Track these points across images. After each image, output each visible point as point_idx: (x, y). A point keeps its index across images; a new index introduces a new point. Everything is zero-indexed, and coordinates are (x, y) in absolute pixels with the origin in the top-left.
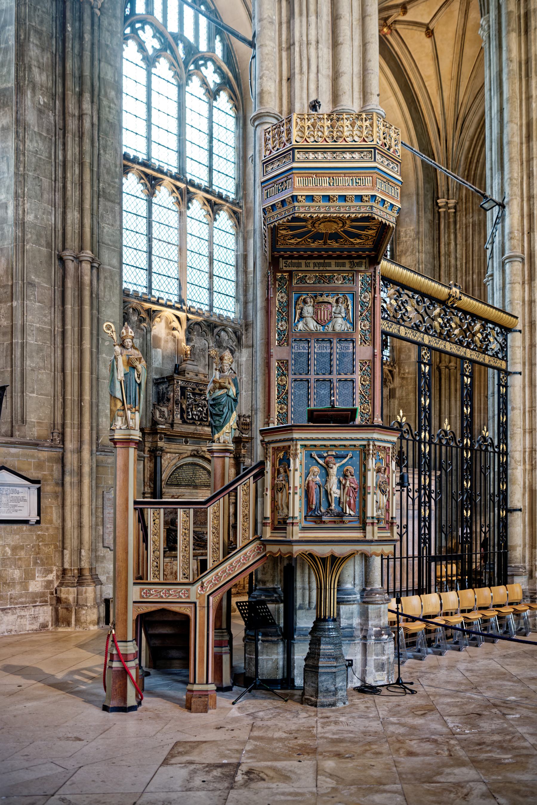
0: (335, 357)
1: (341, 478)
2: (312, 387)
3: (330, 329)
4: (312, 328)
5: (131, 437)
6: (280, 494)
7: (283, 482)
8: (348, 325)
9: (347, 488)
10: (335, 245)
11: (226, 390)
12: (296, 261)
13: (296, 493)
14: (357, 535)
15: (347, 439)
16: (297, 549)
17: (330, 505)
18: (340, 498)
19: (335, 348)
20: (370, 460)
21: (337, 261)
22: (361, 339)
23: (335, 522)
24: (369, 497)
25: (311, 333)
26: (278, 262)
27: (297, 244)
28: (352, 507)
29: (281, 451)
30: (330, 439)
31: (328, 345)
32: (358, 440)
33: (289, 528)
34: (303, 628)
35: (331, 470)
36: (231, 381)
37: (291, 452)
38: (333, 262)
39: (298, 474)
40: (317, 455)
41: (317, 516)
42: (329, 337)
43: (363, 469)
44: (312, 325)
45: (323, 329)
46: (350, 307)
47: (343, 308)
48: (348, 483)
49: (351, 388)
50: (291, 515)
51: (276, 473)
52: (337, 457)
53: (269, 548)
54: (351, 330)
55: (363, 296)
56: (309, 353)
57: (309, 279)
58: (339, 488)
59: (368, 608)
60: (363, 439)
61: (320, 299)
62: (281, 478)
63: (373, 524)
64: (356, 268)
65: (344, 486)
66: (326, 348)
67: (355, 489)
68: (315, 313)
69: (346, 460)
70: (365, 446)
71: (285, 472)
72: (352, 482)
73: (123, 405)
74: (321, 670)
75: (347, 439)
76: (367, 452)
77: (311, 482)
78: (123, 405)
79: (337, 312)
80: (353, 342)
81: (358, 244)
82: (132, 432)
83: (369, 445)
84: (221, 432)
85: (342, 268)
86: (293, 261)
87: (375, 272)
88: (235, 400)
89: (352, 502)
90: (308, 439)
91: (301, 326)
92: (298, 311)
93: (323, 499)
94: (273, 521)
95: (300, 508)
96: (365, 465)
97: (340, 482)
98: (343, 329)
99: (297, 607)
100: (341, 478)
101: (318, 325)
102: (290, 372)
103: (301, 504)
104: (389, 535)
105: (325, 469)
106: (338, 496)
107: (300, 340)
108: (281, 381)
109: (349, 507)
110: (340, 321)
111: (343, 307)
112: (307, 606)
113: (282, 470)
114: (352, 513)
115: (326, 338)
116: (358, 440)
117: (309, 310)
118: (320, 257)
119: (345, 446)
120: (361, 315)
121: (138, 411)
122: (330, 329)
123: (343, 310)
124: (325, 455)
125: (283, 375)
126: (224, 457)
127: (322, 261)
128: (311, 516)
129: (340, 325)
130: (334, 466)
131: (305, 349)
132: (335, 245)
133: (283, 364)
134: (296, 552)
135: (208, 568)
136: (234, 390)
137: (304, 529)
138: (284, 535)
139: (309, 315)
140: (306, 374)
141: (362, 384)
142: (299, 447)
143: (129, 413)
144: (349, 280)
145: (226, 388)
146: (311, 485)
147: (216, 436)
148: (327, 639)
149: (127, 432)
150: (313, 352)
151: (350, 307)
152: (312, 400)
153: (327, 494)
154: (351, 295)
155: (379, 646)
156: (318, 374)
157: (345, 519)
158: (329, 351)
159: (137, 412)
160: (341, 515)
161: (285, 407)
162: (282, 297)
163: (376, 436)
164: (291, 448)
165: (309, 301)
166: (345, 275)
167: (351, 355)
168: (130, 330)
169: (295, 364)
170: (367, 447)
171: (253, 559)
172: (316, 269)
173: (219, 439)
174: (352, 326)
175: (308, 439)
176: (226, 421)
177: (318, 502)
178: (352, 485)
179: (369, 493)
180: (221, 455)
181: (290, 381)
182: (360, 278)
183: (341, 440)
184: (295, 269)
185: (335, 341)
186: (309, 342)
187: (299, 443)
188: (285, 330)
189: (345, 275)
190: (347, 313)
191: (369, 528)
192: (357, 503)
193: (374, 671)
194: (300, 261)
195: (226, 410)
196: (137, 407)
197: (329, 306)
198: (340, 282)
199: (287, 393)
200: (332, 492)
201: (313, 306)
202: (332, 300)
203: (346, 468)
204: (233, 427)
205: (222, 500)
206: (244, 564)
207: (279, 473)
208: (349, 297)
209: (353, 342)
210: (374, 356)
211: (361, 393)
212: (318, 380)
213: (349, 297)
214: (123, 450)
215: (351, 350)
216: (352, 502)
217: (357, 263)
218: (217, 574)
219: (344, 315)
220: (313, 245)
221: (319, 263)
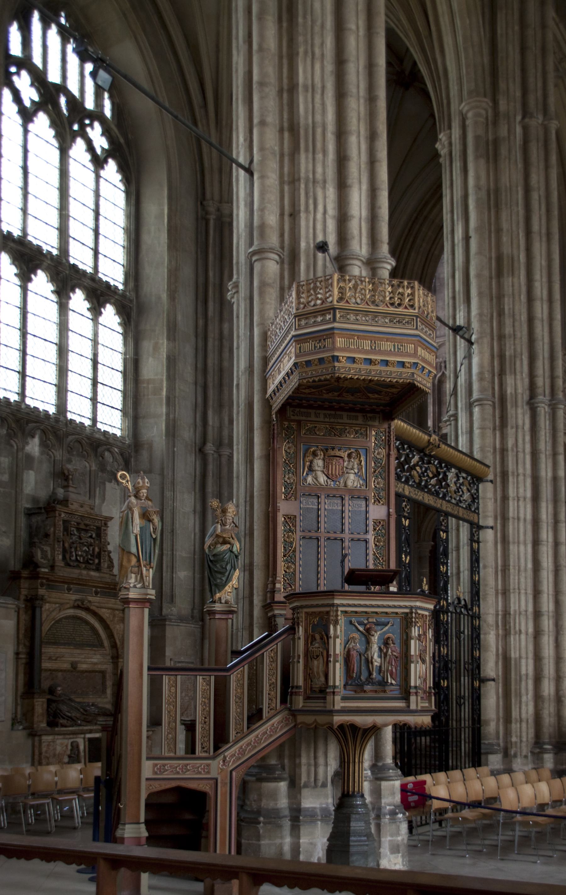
0: (346, 514)
1: (382, 646)
2: (322, 546)
4: (322, 482)
6: (316, 662)
7: (321, 649)
8: (361, 482)
9: (388, 657)
10: (350, 398)
11: (229, 546)
12: (305, 410)
13: (338, 661)
14: (400, 704)
15: (389, 607)
16: (338, 719)
17: (370, 674)
18: (380, 667)
19: (347, 505)
20: (413, 629)
21: (349, 414)
22: (375, 496)
23: (376, 691)
24: (413, 666)
25: (321, 488)
27: (309, 394)
28: (394, 676)
29: (316, 617)
30: (372, 606)
32: (400, 607)
33: (329, 698)
34: (309, 808)
35: (373, 638)
37: (332, 618)
38: (345, 414)
39: (338, 641)
41: (357, 685)
42: (340, 493)
43: (405, 637)
44: (322, 479)
45: (334, 486)
46: (363, 463)
47: (356, 463)
48: (390, 651)
49: (364, 548)
50: (331, 683)
51: (310, 639)
52: (377, 624)
53: (301, 718)
54: (363, 488)
55: (377, 452)
56: (318, 509)
58: (380, 657)
59: (380, 785)
60: (406, 607)
61: (332, 453)
62: (317, 645)
63: (416, 694)
64: (370, 423)
65: (386, 655)
66: (337, 504)
67: (397, 657)
68: (326, 466)
69: (387, 628)
70: (407, 613)
71: (322, 638)
72: (395, 649)
74: (352, 850)
75: (389, 607)
76: (409, 620)
77: (352, 650)
80: (366, 500)
81: (376, 399)
83: (412, 613)
84: (223, 592)
85: (354, 422)
86: (302, 410)
87: (389, 428)
89: (394, 670)
90: (349, 606)
91: (310, 479)
92: (308, 463)
93: (363, 668)
94: (305, 690)
95: (340, 676)
96: (407, 634)
97: (380, 649)
99: (302, 784)
100: (382, 646)
101: (328, 480)
103: (340, 673)
104: (427, 705)
105: (365, 636)
106: (378, 665)
107: (309, 495)
108: (288, 537)
109: (391, 677)
110: (352, 476)
111: (356, 462)
112: (313, 784)
113: (317, 636)
114: (393, 682)
115: (338, 493)
116: (400, 607)
117: (319, 463)
118: (331, 408)
119: (386, 613)
120: (374, 472)
121: (152, 568)
122: (342, 484)
123: (356, 466)
124: (366, 622)
125: (290, 531)
126: (227, 619)
127: (333, 412)
128: (351, 685)
129: (352, 480)
130: (375, 634)
131: (314, 505)
132: (350, 398)
133: (290, 519)
134: (336, 723)
135: (231, 741)
136: (238, 546)
137: (344, 699)
138: (322, 705)
139: (319, 469)
140: (316, 532)
141: (376, 545)
142: (339, 613)
143: (144, 569)
144: (361, 434)
145: (229, 543)
146: (352, 653)
147: (218, 595)
148: (357, 816)
149: (143, 591)
150: (323, 509)
151: (363, 463)
152: (322, 559)
153: (369, 662)
154: (364, 451)
155: (394, 826)
156: (328, 532)
157: (388, 688)
160: (383, 683)
161: (293, 566)
162: (289, 448)
163: (418, 604)
164: (331, 614)
165: (319, 454)
166: (357, 429)
167: (364, 513)
168: (146, 480)
169: (303, 520)
170: (409, 615)
171: (281, 730)
172: (327, 420)
173: (220, 599)
174: (365, 483)
175: (349, 606)
176: (229, 579)
177: (359, 670)
178: (395, 654)
179: (413, 662)
180: (224, 617)
181: (298, 538)
182: (373, 433)
183: (384, 606)
184: (304, 418)
185: (347, 498)
186: (318, 497)
187: (340, 609)
188: (292, 483)
189: (357, 429)
190: (360, 469)
191: (413, 698)
192: (398, 672)
193: (388, 853)
195: (229, 567)
197: (341, 461)
198: (352, 436)
199: (294, 551)
200: (374, 660)
201: (324, 460)
203: (386, 636)
204: (235, 586)
205: (246, 667)
206: (271, 736)
207: (314, 639)
208: (362, 452)
209: (366, 500)
210: (389, 515)
211: (374, 554)
212: (329, 539)
213: (362, 452)
214: (137, 610)
216: (394, 670)
217: (370, 417)
218: (241, 747)
219: (356, 471)
220: (325, 396)
221: (330, 415)
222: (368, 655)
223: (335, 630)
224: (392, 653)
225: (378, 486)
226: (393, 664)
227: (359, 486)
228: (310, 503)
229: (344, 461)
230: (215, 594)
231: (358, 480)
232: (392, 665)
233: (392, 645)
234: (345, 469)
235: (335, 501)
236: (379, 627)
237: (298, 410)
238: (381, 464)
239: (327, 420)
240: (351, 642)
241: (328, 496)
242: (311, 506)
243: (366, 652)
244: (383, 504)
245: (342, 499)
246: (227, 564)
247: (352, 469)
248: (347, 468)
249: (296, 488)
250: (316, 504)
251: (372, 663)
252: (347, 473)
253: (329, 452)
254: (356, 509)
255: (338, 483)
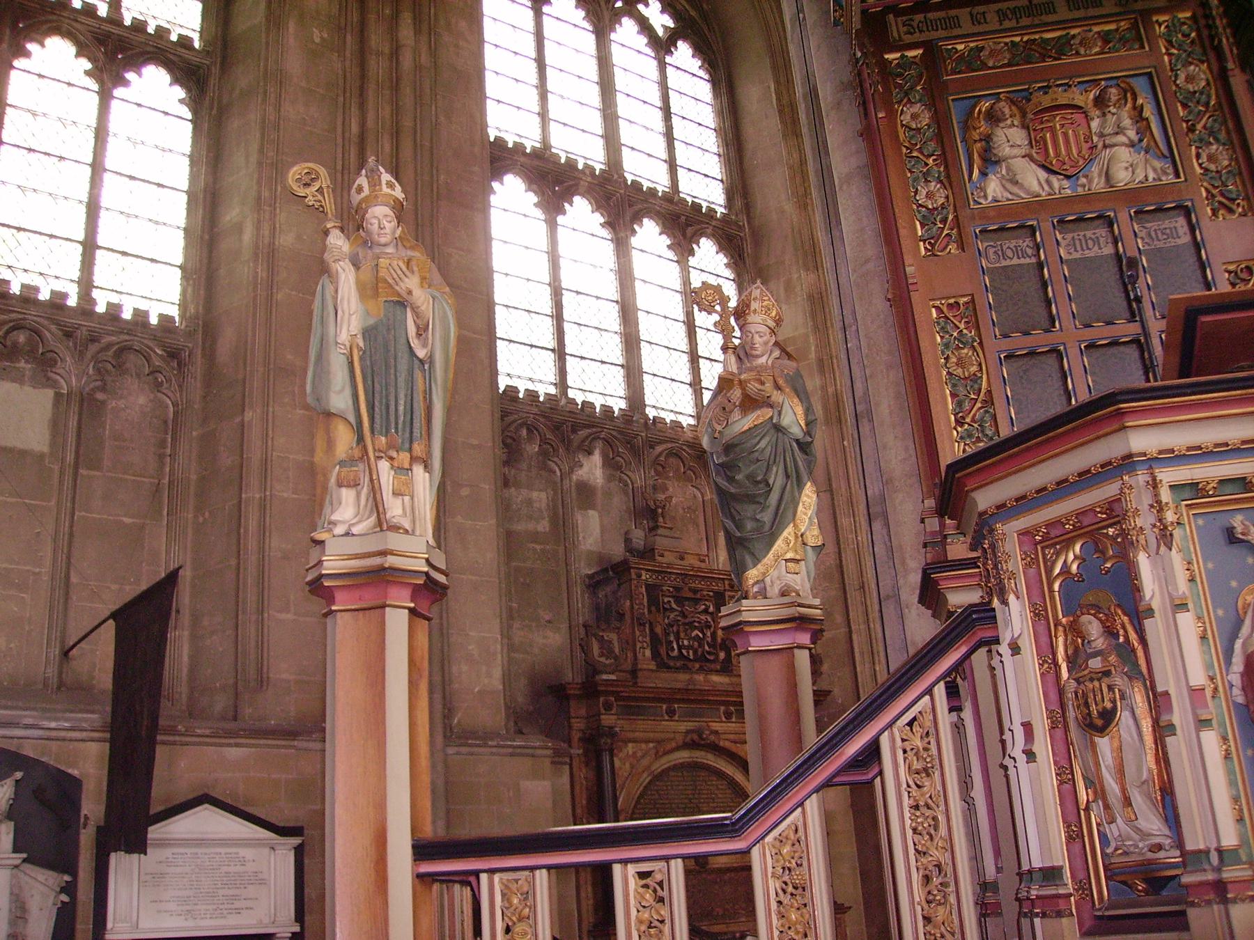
3: (1098, 184)
4: (1035, 187)
5: (391, 561)
8: (1158, 164)
11: (767, 413)
12: (941, 14)
22: (1210, 196)
26: (885, 26)
31: (1102, 232)
36: (781, 382)
44: (1033, 179)
54: (1170, 178)
56: (1040, 266)
57: (993, 53)
66: (1096, 241)
68: (1036, 142)
73: (361, 439)
78: (361, 439)
79: (1108, 130)
82: (394, 541)
86: (930, 15)
88: (804, 447)
98: (1141, 177)
102: (988, 332)
110: (1124, 154)
120: (1191, 129)
123: (1127, 122)
131: (1025, 255)
136: (800, 410)
140: (1047, 331)
145: (767, 403)
150: (1053, 260)
158: (1108, 250)
159: (418, 470)
165: (1007, 111)
181: (993, 358)
185: (1123, 217)
186: (1032, 230)
188: (943, 206)
194: (953, 13)
196: (418, 449)
198: (1097, 49)
199: (989, 401)
201: (1025, 126)
202: (1085, 99)
209: (1187, 212)
212: (1091, 346)
213: (1140, 85)
215: (1186, 239)
219: (1132, 134)
225: (1212, 167)
227: (1151, 176)
228: (1010, 253)
229: (1088, 119)
230: (745, 569)
231: (1146, 161)
234: (1095, 139)
235: (1089, 234)
237: (919, 17)
238: (1207, 104)
239: (1007, 24)
241: (1061, 222)
242: (1015, 261)
244: (1244, 215)
245: (1110, 223)
246: (768, 469)
247: (1120, 131)
248: (1101, 135)
249: (956, 217)
250: (1029, 251)
252: (1105, 147)
253: (1034, 100)
254: (1160, 245)
255: (1083, 180)
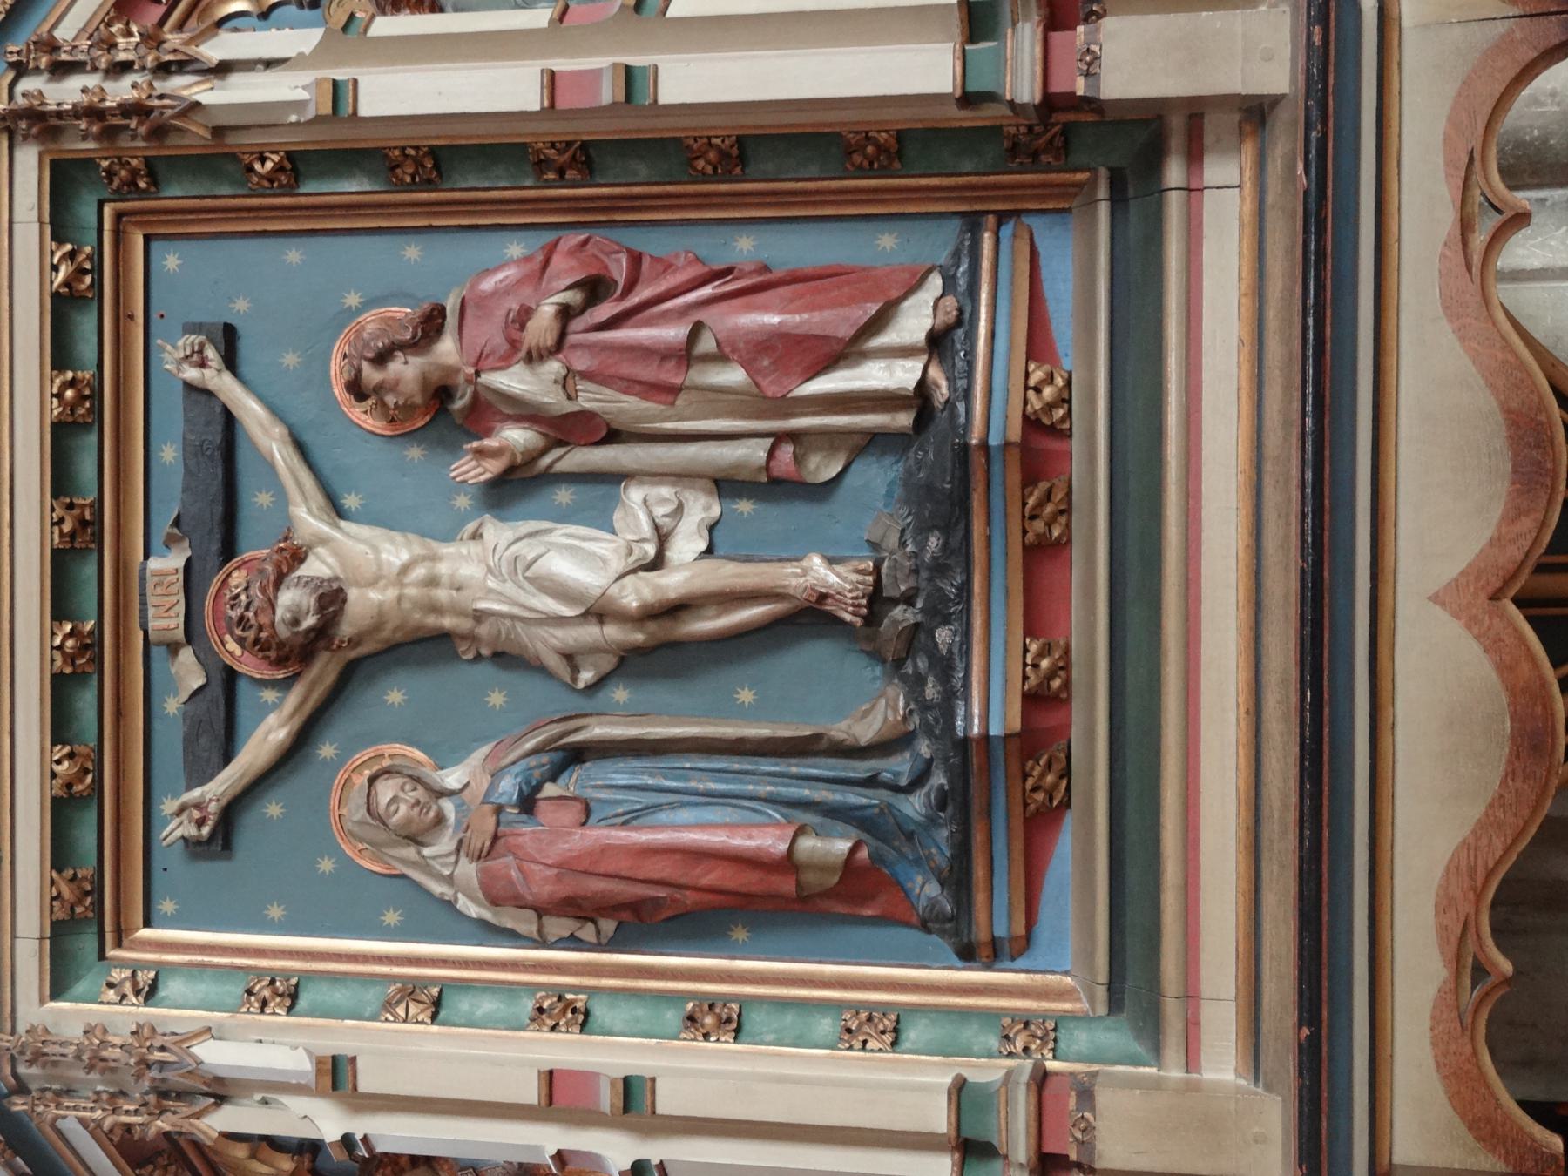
9: (590, 398)
18: (725, 485)
35: (363, 603)
40: (199, 774)
43: (353, 186)
48: (513, 380)
67: (595, 288)
69: (250, 410)
96: (297, 165)
100: (471, 470)
106: (701, 508)
200: (635, 593)
222: (571, 658)
223: (272, 1087)
224: (534, 358)
226: (674, 333)
232: (686, 354)
233: (447, 348)
236: (255, 500)
240: (424, 866)
243: (541, 669)
251: (676, 609)
